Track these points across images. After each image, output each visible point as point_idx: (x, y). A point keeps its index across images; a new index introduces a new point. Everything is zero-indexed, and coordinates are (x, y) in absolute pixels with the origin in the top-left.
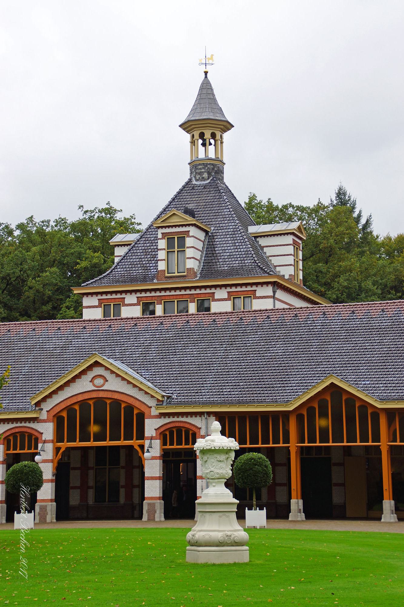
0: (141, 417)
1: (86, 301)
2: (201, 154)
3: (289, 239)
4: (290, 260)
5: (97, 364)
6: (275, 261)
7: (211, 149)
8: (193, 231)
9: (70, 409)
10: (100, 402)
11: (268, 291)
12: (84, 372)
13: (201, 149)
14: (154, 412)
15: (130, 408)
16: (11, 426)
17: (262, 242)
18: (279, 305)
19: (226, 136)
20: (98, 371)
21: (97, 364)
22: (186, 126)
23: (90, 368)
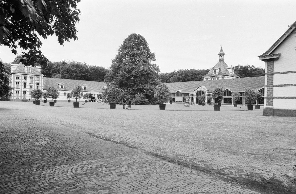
0: (205, 93)
1: (204, 78)
2: (221, 58)
3: (231, 69)
4: (232, 72)
5: (200, 87)
6: (229, 72)
7: (222, 57)
8: (217, 69)
9: (197, 92)
10: (201, 91)
11: (226, 76)
12: (199, 87)
13: (221, 57)
14: (207, 92)
15: (204, 92)
16: (191, 94)
17: (228, 69)
18: (228, 78)
19: (224, 55)
20: (200, 87)
21: (200, 87)
22: (219, 54)
23: (199, 87)
